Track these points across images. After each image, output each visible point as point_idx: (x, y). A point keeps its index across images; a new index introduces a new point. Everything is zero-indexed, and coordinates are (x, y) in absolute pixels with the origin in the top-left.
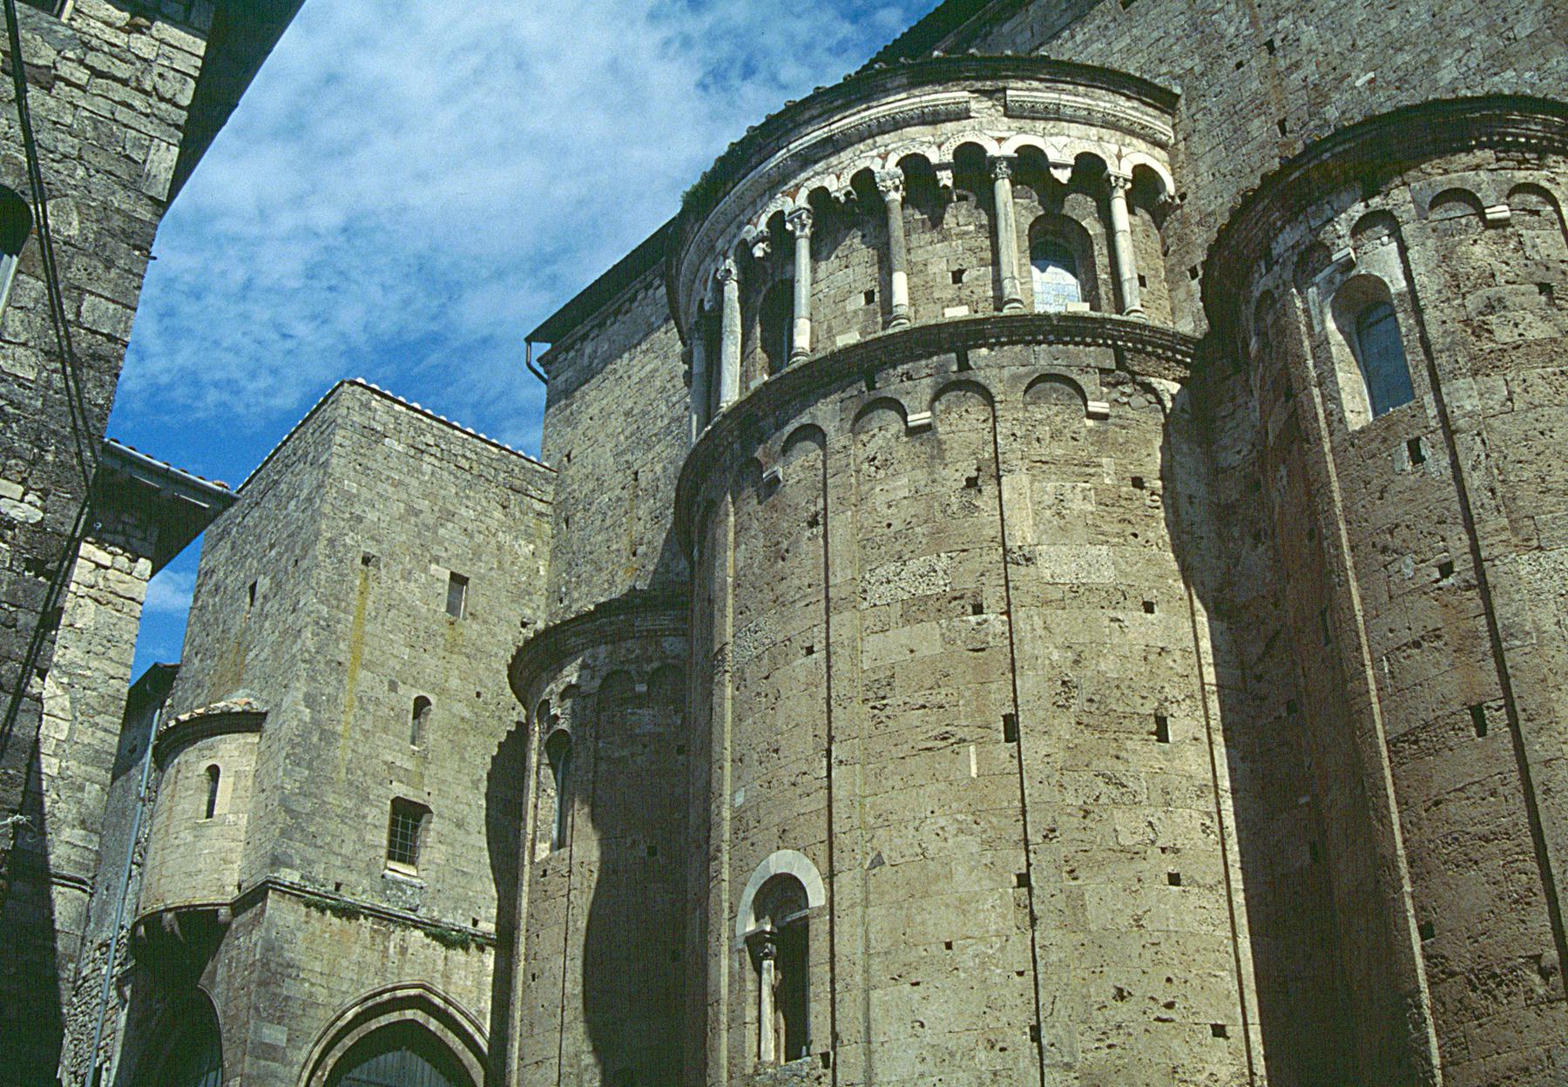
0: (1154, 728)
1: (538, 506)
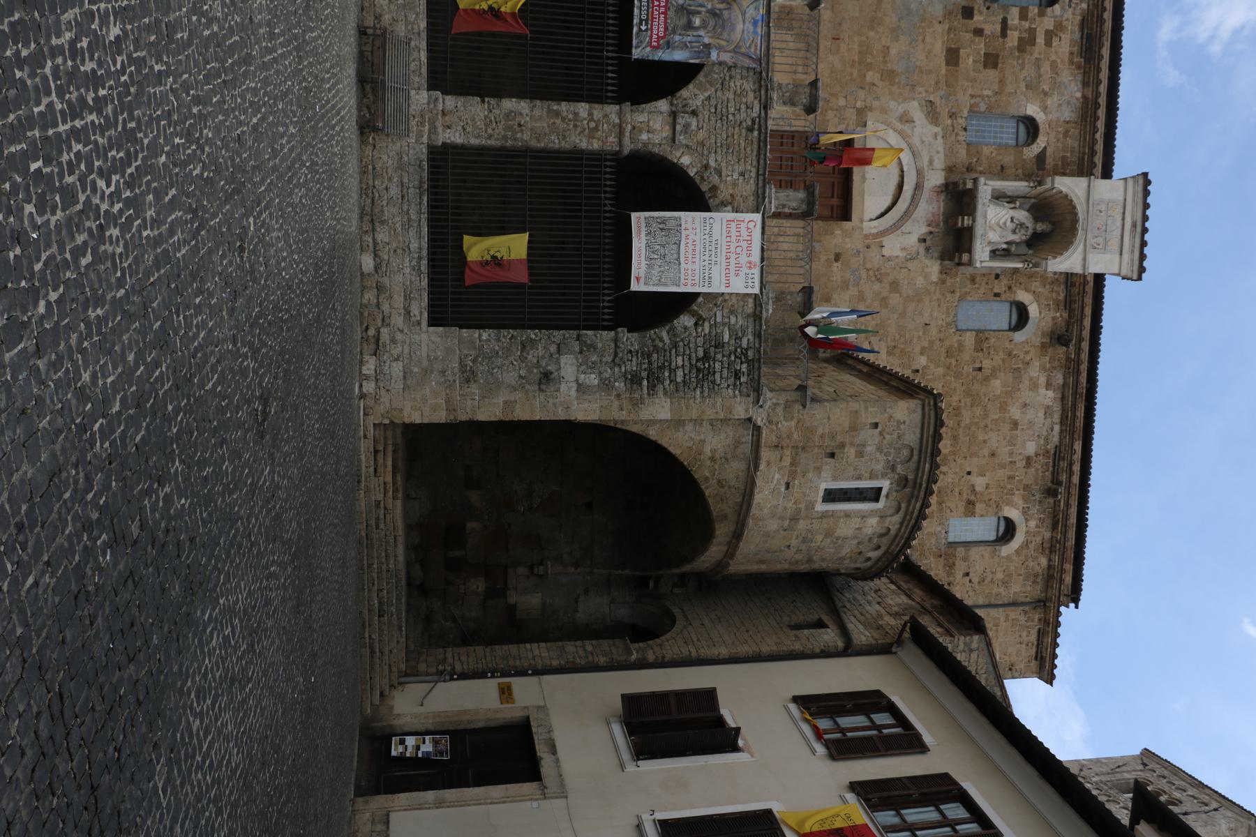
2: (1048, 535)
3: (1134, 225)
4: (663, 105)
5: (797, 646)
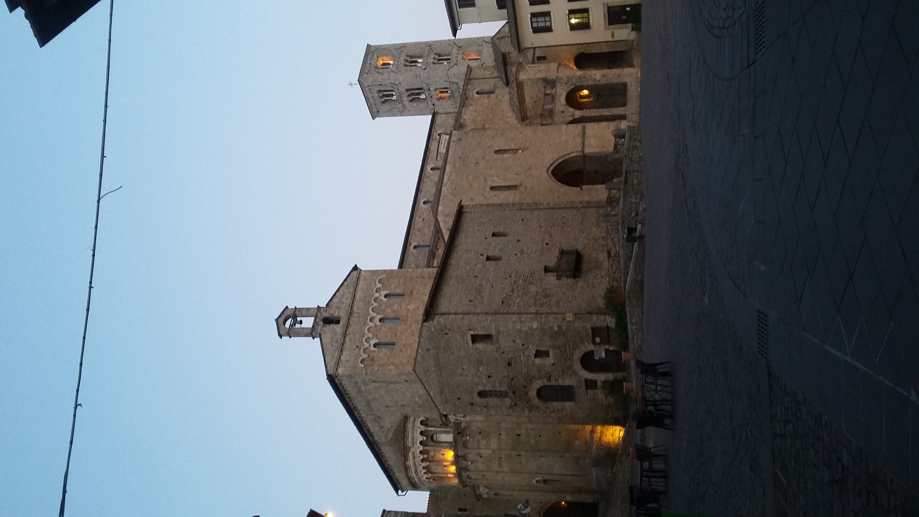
0: (518, 436)
1: (439, 493)
2: (467, 92)
3: (441, 144)
4: (576, 117)
5: (546, 48)
